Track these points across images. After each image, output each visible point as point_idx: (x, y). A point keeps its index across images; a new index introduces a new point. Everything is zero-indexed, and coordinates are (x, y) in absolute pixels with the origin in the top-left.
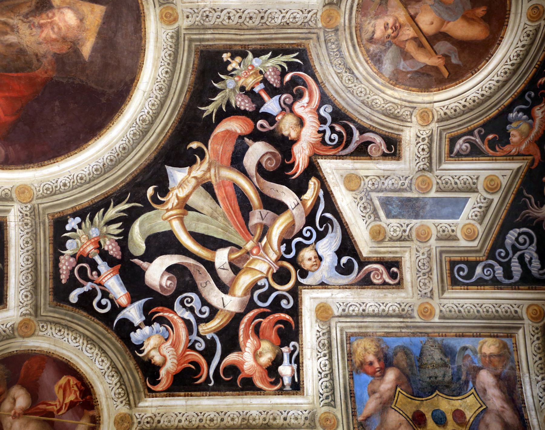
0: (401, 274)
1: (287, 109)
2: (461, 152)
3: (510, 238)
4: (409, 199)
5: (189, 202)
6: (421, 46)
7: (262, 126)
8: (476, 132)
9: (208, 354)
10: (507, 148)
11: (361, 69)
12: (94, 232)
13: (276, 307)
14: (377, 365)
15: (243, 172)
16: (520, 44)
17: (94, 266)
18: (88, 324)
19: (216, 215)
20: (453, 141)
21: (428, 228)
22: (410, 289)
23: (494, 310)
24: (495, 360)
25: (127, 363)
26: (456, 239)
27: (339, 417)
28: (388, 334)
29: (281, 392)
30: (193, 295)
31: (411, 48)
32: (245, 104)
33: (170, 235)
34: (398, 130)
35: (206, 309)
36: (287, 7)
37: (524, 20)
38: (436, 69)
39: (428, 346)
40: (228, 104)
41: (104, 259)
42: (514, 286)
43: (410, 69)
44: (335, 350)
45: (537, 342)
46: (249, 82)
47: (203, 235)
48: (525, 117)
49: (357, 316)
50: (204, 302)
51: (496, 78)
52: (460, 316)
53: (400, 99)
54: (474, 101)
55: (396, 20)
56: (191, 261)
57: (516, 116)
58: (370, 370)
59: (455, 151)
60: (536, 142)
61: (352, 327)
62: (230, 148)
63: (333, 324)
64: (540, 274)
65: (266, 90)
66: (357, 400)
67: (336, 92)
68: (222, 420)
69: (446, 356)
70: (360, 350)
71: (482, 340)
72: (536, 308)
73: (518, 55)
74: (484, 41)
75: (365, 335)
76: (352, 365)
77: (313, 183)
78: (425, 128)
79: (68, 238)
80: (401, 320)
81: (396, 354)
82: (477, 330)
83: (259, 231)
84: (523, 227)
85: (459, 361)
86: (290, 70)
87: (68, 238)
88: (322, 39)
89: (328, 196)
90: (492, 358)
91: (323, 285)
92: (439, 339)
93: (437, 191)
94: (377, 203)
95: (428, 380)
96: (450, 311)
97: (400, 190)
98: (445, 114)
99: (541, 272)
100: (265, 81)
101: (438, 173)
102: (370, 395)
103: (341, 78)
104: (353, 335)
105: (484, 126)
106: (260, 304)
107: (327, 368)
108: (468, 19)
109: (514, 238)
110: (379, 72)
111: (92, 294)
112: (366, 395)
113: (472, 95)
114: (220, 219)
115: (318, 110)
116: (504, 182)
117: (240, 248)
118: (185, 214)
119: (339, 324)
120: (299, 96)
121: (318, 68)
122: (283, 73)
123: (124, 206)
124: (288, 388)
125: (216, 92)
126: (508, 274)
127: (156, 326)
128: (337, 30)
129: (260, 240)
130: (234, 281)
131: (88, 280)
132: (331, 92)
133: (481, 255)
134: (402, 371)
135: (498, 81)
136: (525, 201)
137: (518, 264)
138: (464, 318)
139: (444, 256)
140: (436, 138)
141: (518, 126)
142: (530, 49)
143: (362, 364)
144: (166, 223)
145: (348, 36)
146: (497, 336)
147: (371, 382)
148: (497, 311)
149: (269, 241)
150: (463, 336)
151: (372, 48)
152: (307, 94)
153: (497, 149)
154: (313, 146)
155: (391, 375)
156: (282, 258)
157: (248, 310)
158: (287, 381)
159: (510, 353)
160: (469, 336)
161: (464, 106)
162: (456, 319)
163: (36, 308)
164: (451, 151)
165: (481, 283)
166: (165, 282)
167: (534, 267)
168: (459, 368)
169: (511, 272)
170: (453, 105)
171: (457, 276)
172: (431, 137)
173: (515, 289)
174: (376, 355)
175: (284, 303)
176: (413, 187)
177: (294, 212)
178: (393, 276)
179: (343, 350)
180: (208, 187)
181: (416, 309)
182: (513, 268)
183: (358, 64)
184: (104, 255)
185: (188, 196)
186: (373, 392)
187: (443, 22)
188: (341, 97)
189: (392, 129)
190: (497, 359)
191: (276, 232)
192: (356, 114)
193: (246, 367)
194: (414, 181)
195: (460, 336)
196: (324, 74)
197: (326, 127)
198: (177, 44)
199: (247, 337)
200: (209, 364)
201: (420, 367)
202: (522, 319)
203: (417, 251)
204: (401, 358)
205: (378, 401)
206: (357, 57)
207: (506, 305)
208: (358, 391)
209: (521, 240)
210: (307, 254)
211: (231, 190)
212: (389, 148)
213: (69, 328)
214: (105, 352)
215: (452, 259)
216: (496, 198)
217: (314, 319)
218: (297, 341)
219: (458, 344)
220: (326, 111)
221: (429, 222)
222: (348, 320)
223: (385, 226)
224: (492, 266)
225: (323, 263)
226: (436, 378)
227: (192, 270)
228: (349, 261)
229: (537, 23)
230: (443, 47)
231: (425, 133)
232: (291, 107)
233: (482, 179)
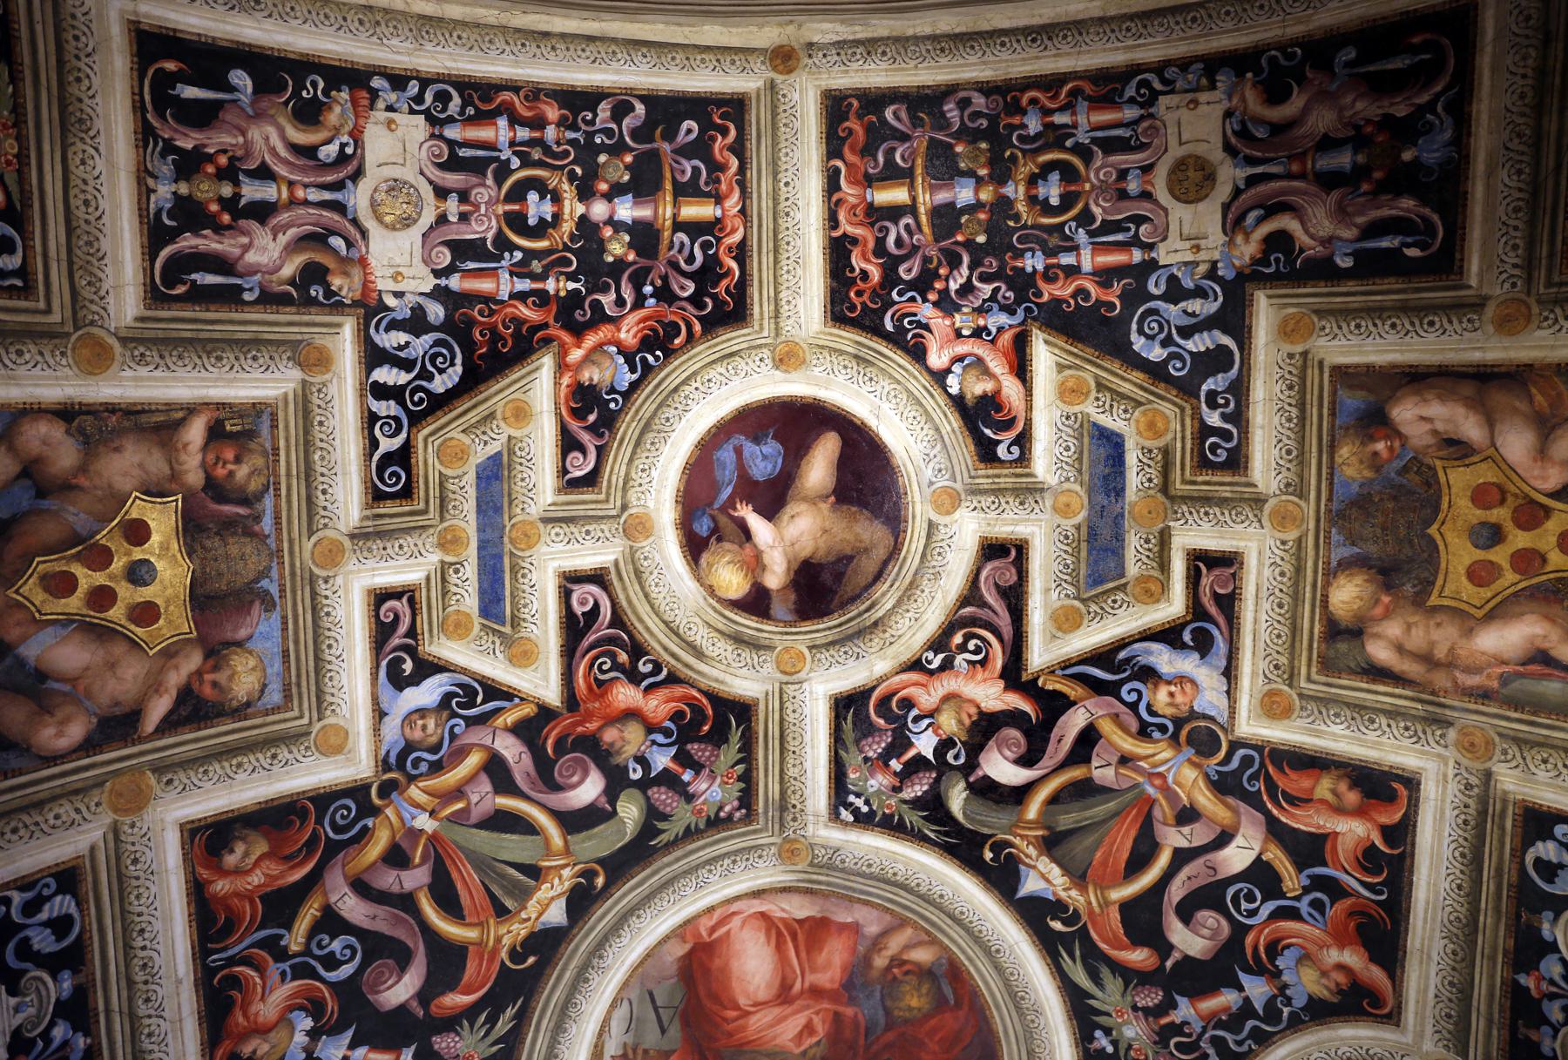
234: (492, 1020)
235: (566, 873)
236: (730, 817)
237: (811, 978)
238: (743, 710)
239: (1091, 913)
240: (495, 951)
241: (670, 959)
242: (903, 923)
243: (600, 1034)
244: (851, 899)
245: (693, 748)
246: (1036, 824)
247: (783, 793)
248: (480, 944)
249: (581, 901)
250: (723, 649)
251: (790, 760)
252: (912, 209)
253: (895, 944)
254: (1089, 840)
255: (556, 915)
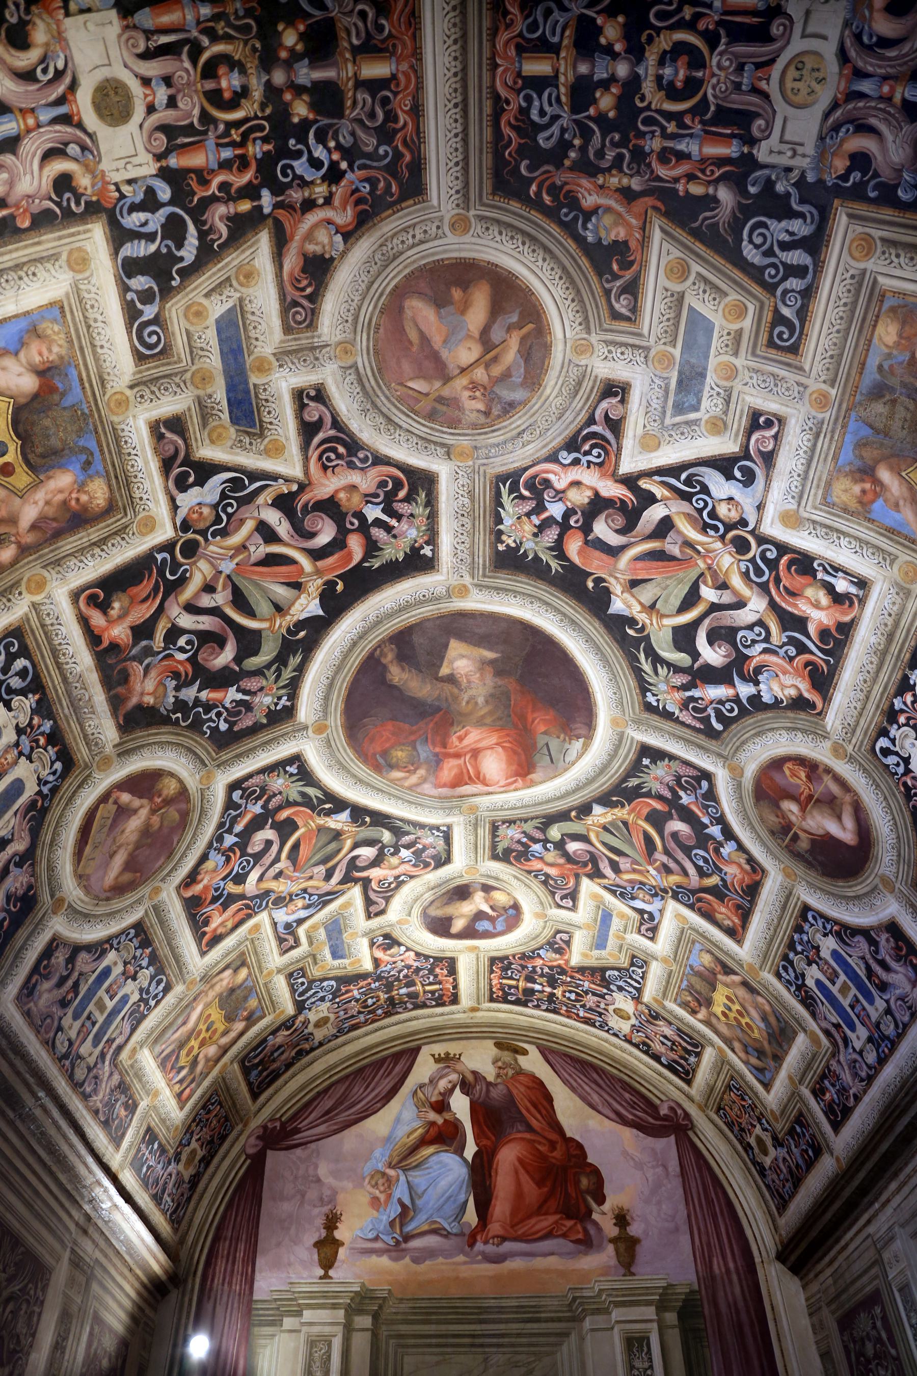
0: (768, 413)
1: (560, 495)
2: (631, 307)
3: (754, 256)
4: (680, 382)
5: (648, 604)
6: (495, 359)
7: (577, 522)
8: (607, 286)
9: (802, 649)
10: (633, 244)
11: (519, 423)
12: (663, 687)
13: (772, 565)
14: (867, 486)
15: (623, 548)
16: (498, 238)
17: (693, 699)
18: (744, 728)
19: (663, 585)
20: (616, 316)
21: (719, 364)
22: (789, 410)
23: (842, 309)
24: (908, 330)
25: (788, 718)
26: (740, 333)
27: (909, 558)
28: (836, 458)
29: (862, 601)
30: (740, 634)
31: (497, 371)
32: (552, 534)
33: (676, 630)
34: (595, 381)
35: (757, 629)
36: (452, 493)
37: (467, 238)
38: (523, 340)
39: (863, 414)
40: (551, 549)
41: (689, 690)
42: (819, 266)
43: (522, 370)
44: (836, 525)
45: (902, 259)
46: (528, 528)
47: (682, 602)
48: (594, 219)
49: (803, 486)
50: (750, 627)
51: (540, 263)
52: (837, 359)
53: (558, 378)
54: (567, 288)
55: (466, 388)
56: (707, 622)
57: (592, 231)
58: (870, 496)
59: (628, 314)
60: (629, 204)
61: (815, 495)
62: (597, 554)
63: (806, 515)
64: (812, 222)
65: (538, 514)
66: (899, 529)
67: (544, 446)
68: (868, 672)
69: (883, 396)
70: (845, 498)
71: (875, 340)
72: (855, 244)
73: (512, 238)
74: (491, 286)
75: (829, 485)
76: (859, 514)
77: (644, 484)
78: (596, 350)
79: (664, 707)
80: (822, 435)
81: (862, 458)
82: (862, 343)
83: (689, 551)
84: (742, 234)
85: (894, 382)
86: (518, 490)
87: (664, 707)
88: (485, 461)
89: (660, 471)
90: (904, 335)
91: (760, 507)
92: (858, 397)
93: (674, 346)
94: (678, 419)
95: (905, 432)
96: (828, 369)
97: (667, 392)
98: (580, 324)
99: (809, 220)
100: (528, 515)
101: (652, 339)
102: (899, 511)
103: (529, 442)
104: (824, 498)
105: (600, 275)
106: (765, 578)
107: (854, 542)
108: (464, 308)
109: (755, 251)
110: (524, 403)
111: (719, 714)
112: (897, 516)
113: (559, 292)
114: (668, 582)
115: (564, 466)
116: (676, 253)
117: (702, 574)
118: (658, 612)
119: (808, 509)
120: (547, 483)
121: (516, 465)
122: (522, 497)
123: (642, 657)
124: (861, 593)
125: (537, 558)
126: (799, 271)
127: (760, 678)
128: (476, 447)
129: (699, 552)
130: (735, 592)
131: (705, 710)
132: (544, 452)
133: (767, 302)
134: (883, 459)
135: (544, 260)
136: (707, 226)
137: (791, 253)
138: (841, 355)
139: (759, 352)
140: (609, 337)
141: (606, 228)
142: (504, 223)
143: (860, 502)
144: (664, 629)
145: (483, 437)
146: (878, 316)
147: (886, 501)
148: (845, 304)
149: (701, 544)
150: (864, 364)
151: (495, 412)
152: (545, 475)
153: (632, 258)
154: (603, 475)
155: (885, 475)
156: (722, 537)
157: (768, 593)
158: (853, 590)
159: (905, 306)
160: (866, 356)
161: (573, 301)
162: (839, 365)
163: (720, 755)
164: (628, 319)
165: (803, 313)
166: (722, 651)
167: (799, 229)
168: (904, 385)
169: (798, 265)
170: (571, 315)
171: (787, 344)
172: (607, 343)
173: (822, 267)
174: (855, 481)
175: (771, 555)
176: (665, 375)
177: (673, 510)
178: (769, 424)
179: (839, 516)
180: (634, 584)
181: (814, 413)
182: (795, 263)
183: (513, 426)
184: (684, 688)
185: (641, 603)
186: (897, 505)
187: (469, 337)
188: (551, 441)
189: (593, 388)
190: (907, 328)
191: (693, 534)
192: (572, 426)
193: (825, 622)
194: (657, 373)
195: (862, 369)
196: (524, 459)
197: (584, 459)
198: (488, 587)
199: (796, 606)
200: (812, 653)
201: (886, 435)
202: (864, 271)
203: (746, 384)
204: (869, 454)
205: (908, 505)
206: (505, 427)
207: (840, 289)
208: (889, 522)
209: (758, 240)
210: (723, 510)
211: (640, 565)
212: (616, 394)
213: (743, 743)
214: (773, 729)
215: (765, 342)
216: (696, 268)
217: (794, 532)
218: (815, 559)
219: (871, 375)
220: (566, 458)
221: (713, 362)
222: (806, 497)
223: (707, 416)
224: (785, 292)
225: (737, 498)
226: (906, 420)
227: (715, 624)
228: (740, 469)
229: (473, 220)
230: (497, 334)
231: (602, 350)
232: (558, 492)
233: (669, 285)
234: (639, 787)
235: (590, 822)
236: (504, 823)
237: (461, 761)
238: (495, 857)
239: (312, 818)
240: (632, 811)
241: (541, 774)
242: (410, 788)
243: (583, 754)
244: (440, 798)
245: (520, 848)
246: (345, 839)
247: (476, 830)
248: (638, 817)
249: (585, 810)
250: (505, 878)
251: (472, 841)
252: (423, 985)
253: (414, 779)
254: (319, 845)
255: (597, 809)
